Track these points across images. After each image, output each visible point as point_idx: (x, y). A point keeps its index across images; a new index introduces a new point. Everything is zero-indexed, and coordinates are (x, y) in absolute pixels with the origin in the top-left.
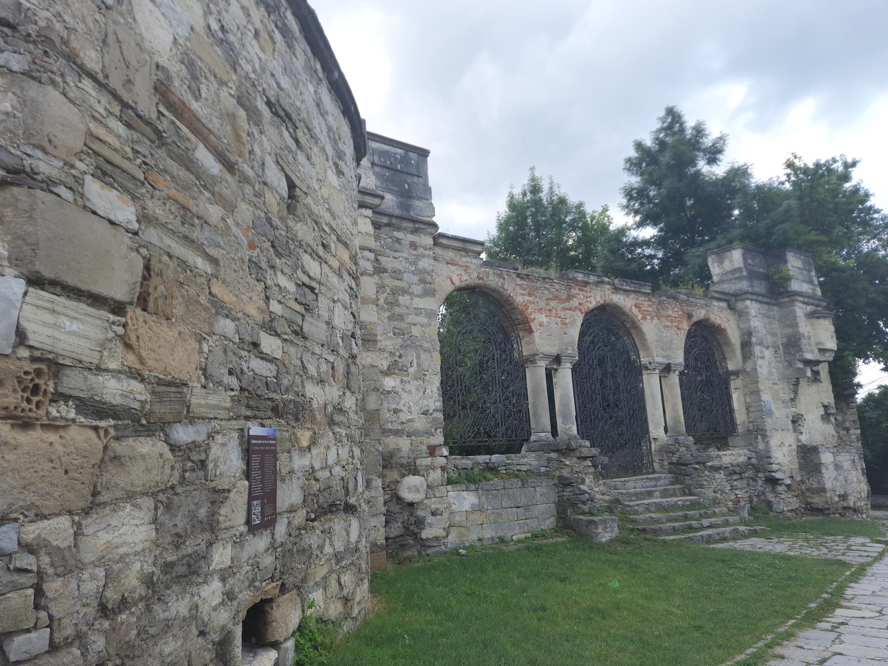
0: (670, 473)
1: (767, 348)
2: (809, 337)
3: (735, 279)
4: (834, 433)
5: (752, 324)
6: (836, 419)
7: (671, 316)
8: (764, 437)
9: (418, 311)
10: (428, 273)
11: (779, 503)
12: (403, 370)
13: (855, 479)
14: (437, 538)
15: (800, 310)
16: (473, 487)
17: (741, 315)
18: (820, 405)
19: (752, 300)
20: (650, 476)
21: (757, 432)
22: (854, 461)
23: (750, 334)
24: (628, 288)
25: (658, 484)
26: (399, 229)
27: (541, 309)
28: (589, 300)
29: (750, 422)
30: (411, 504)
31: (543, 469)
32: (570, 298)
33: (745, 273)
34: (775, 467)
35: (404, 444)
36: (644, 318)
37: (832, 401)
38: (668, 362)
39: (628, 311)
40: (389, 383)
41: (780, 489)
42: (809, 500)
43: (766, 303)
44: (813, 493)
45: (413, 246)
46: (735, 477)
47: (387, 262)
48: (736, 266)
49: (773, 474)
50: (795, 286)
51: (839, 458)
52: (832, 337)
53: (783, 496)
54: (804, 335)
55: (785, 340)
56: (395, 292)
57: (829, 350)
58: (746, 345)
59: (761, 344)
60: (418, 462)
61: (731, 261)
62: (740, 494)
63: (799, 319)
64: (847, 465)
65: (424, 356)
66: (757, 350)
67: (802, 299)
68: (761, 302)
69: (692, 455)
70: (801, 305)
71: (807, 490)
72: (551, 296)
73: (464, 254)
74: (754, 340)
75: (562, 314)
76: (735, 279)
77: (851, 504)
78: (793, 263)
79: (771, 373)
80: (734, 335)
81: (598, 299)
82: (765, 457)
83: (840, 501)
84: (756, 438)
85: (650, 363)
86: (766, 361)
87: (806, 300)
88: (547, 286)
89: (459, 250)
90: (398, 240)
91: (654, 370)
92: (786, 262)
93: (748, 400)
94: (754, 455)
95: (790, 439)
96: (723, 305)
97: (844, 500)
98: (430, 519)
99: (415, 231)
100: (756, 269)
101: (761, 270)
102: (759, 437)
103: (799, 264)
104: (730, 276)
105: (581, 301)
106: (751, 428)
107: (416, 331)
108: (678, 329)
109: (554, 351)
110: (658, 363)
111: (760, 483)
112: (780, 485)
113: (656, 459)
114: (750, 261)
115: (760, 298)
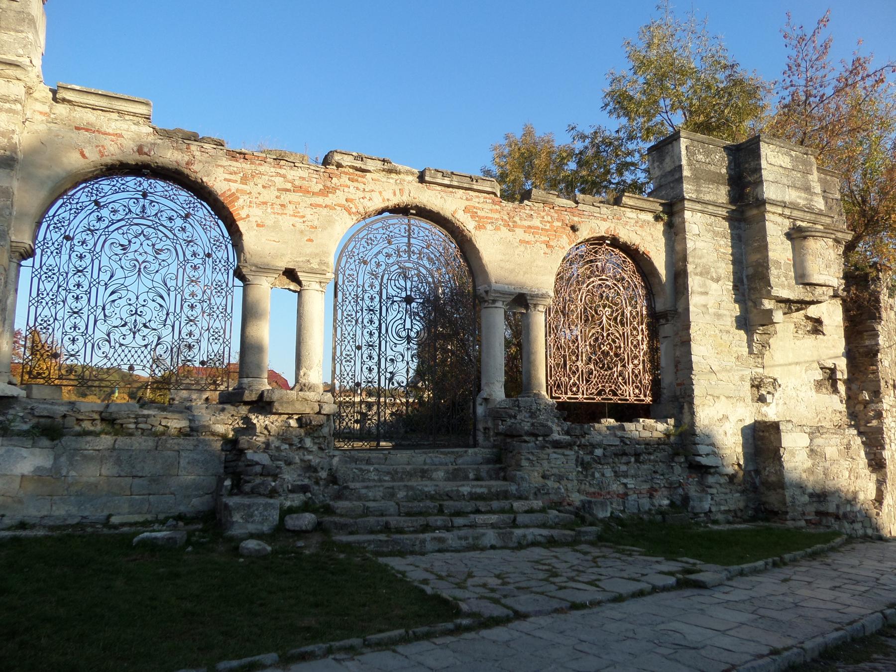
0: (494, 446)
1: (718, 280)
3: (673, 182)
4: (843, 407)
5: (690, 245)
6: (848, 389)
7: (538, 228)
8: (691, 403)
11: (701, 500)
13: (847, 474)
18: (816, 365)
19: (693, 210)
20: (447, 450)
22: (848, 447)
23: (685, 259)
24: (446, 181)
25: (460, 461)
27: (265, 203)
28: (368, 195)
29: (678, 385)
32: (326, 191)
36: (479, 227)
37: (842, 364)
38: (518, 291)
39: (450, 217)
41: (711, 480)
42: (764, 499)
44: (769, 489)
46: (624, 459)
48: (677, 164)
49: (698, 459)
50: (770, 191)
51: (819, 441)
53: (714, 491)
55: (751, 271)
59: (704, 273)
61: (672, 157)
62: (631, 483)
63: (769, 239)
64: (831, 452)
66: (694, 282)
68: (711, 214)
69: (533, 424)
70: (779, 219)
71: (762, 483)
72: (289, 186)
73: (115, 116)
74: (690, 268)
75: (308, 212)
76: (673, 182)
77: (832, 508)
78: (772, 160)
81: (388, 194)
83: (810, 503)
84: (682, 407)
85: (487, 292)
86: (711, 301)
88: (282, 171)
91: (494, 301)
92: (759, 157)
93: (678, 354)
97: (820, 502)
100: (712, 168)
102: (686, 406)
103: (786, 161)
104: (670, 179)
105: (351, 196)
106: (678, 393)
108: (548, 246)
109: (283, 264)
110: (496, 291)
111: (678, 469)
112: (712, 474)
113: (481, 426)
115: (711, 208)
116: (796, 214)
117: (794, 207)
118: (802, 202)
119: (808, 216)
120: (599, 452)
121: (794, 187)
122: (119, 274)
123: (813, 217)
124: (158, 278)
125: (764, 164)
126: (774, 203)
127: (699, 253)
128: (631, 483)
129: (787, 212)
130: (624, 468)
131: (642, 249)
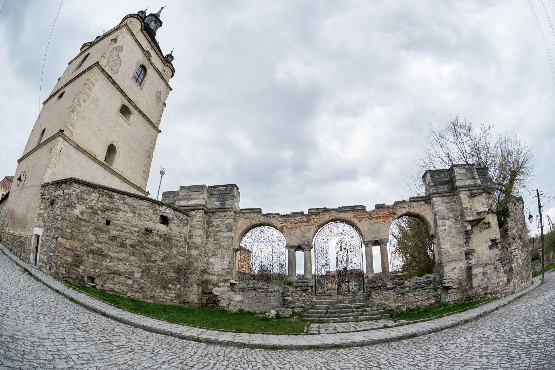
1: (448, 220)
2: (471, 208)
5: (437, 209)
8: (442, 266)
9: (224, 237)
10: (230, 224)
12: (216, 256)
14: (224, 307)
15: (463, 195)
16: (241, 293)
17: (432, 205)
19: (436, 197)
21: (441, 265)
23: (435, 215)
26: (220, 212)
30: (217, 296)
31: (281, 291)
33: (432, 184)
34: (446, 281)
35: (215, 278)
40: (211, 260)
43: (449, 196)
45: (225, 216)
46: (417, 290)
47: (215, 223)
52: (483, 204)
54: (467, 209)
56: (217, 232)
57: (482, 212)
58: (435, 220)
59: (443, 218)
60: (219, 284)
63: (462, 200)
65: (224, 251)
66: (440, 222)
67: (464, 189)
68: (443, 196)
70: (465, 192)
74: (437, 217)
79: (450, 232)
80: (429, 218)
82: (442, 276)
86: (447, 227)
87: (467, 189)
89: (251, 213)
90: (220, 216)
92: (454, 172)
94: (437, 276)
95: (462, 265)
96: (423, 203)
98: (222, 301)
99: (225, 211)
100: (441, 179)
101: (446, 179)
107: (222, 243)
109: (297, 244)
112: (450, 289)
114: (436, 177)
115: (442, 195)
116: (470, 188)
117: (470, 186)
118: (472, 183)
119: (475, 188)
120: (407, 289)
121: (469, 179)
122: (257, 252)
123: (477, 188)
124: (266, 252)
125: (456, 174)
126: (461, 187)
127: (440, 211)
128: (420, 297)
129: (467, 189)
130: (417, 293)
131: (420, 214)
